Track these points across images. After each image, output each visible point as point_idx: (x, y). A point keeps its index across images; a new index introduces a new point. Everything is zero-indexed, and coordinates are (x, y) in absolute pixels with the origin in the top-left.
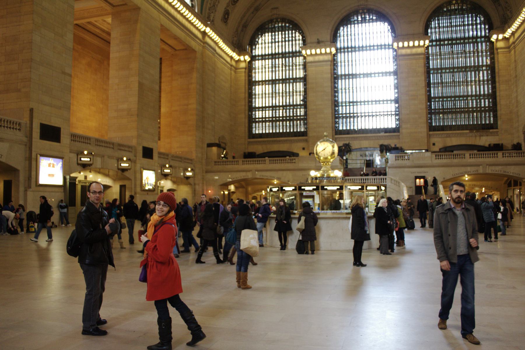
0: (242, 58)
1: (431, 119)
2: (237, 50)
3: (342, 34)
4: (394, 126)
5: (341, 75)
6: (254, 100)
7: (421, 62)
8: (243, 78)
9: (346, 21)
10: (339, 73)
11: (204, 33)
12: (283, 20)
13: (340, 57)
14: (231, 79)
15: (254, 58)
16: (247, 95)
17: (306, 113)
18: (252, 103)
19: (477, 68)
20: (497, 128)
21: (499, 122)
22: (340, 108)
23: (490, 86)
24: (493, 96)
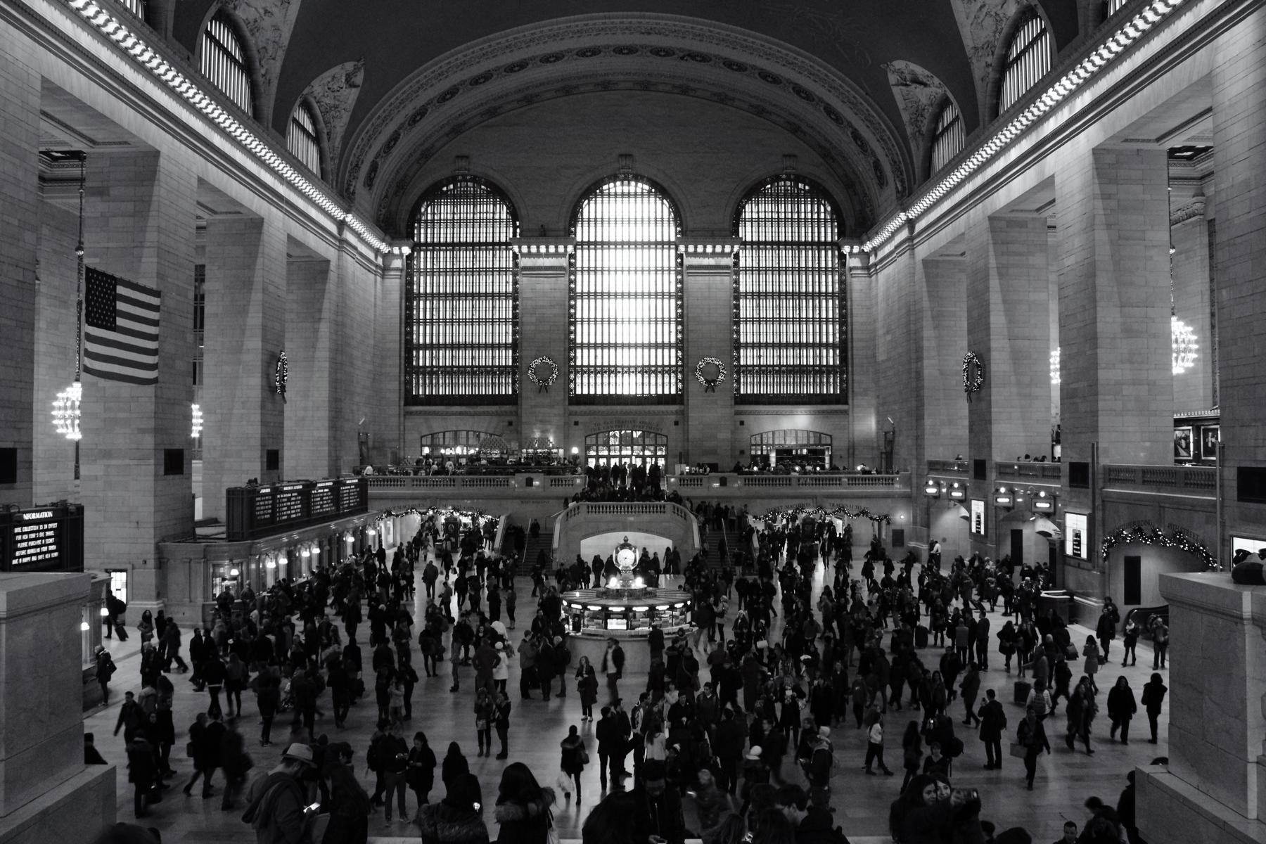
0: (396, 251)
1: (738, 381)
2: (387, 238)
3: (585, 216)
4: (673, 392)
8: (398, 288)
9: (592, 191)
10: (579, 290)
11: (342, 225)
12: (476, 180)
13: (584, 258)
15: (416, 247)
18: (411, 333)
20: (846, 403)
22: (579, 351)
24: (844, 347)
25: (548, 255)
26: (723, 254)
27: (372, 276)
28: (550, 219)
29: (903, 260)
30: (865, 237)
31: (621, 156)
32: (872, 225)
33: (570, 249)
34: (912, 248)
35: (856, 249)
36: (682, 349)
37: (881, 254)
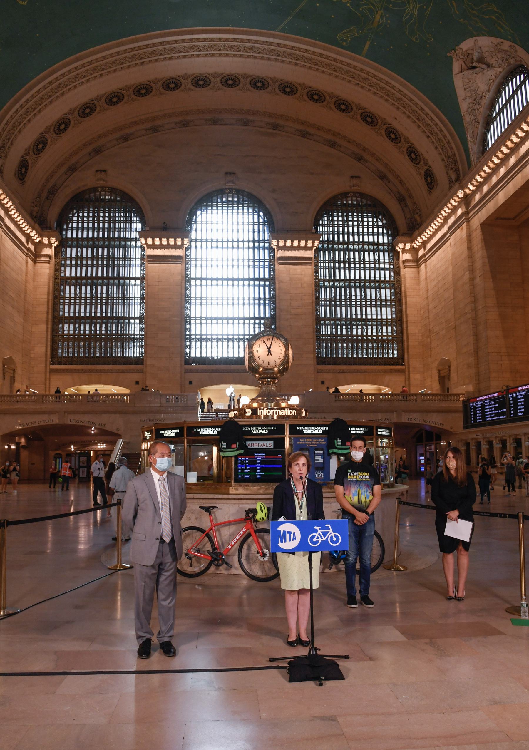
0: (46, 241)
2: (37, 226)
3: (199, 220)
5: (196, 279)
6: (61, 307)
7: (309, 269)
8: (48, 271)
10: (193, 276)
14: (27, 269)
16: (51, 297)
17: (141, 329)
19: (378, 284)
21: (406, 357)
22: (193, 326)
23: (394, 309)
24: (399, 322)
25: (168, 246)
26: (306, 248)
27: (24, 256)
28: (172, 224)
29: (462, 233)
30: (417, 232)
31: (226, 173)
32: (420, 225)
33: (186, 241)
34: (468, 221)
35: (408, 246)
36: (274, 323)
37: (429, 246)
